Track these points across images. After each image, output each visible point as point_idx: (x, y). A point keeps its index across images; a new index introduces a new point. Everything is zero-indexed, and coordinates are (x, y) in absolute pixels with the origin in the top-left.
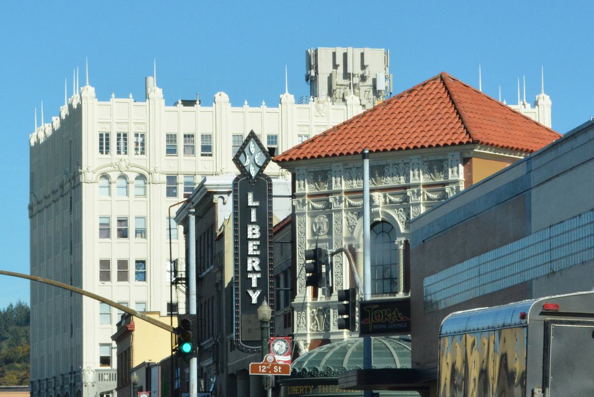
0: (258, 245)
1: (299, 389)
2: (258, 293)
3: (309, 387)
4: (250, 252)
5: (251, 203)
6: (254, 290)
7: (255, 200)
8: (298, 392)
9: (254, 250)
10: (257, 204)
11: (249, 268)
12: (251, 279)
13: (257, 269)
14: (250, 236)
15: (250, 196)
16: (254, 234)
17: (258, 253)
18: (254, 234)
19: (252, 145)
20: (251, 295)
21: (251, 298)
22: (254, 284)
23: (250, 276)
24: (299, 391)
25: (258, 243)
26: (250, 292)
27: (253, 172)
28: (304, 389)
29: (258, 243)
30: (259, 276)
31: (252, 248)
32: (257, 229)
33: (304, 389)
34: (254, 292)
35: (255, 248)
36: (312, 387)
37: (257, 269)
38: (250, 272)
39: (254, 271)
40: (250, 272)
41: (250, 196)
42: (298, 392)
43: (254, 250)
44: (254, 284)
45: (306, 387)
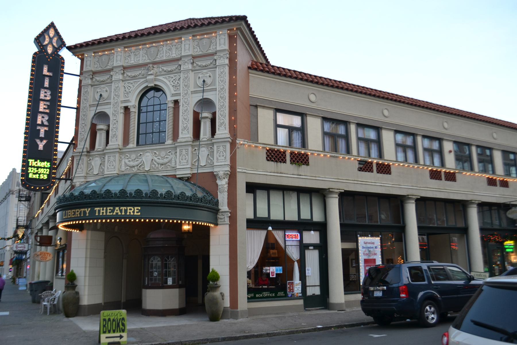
0: (48, 105)
1: (75, 212)
2: (45, 142)
3: (86, 209)
4: (41, 109)
5: (45, 71)
6: (42, 139)
7: (48, 71)
8: (73, 215)
9: (44, 108)
10: (51, 74)
11: (39, 122)
12: (39, 130)
13: (46, 123)
14: (42, 96)
16: (45, 96)
17: (47, 111)
18: (45, 96)
19: (52, 33)
21: (38, 146)
22: (42, 135)
23: (38, 128)
24: (75, 214)
25: (48, 103)
26: (38, 141)
27: (50, 50)
28: (81, 212)
29: (48, 103)
30: (46, 129)
31: (42, 107)
32: (49, 93)
33: (81, 212)
34: (41, 141)
36: (89, 209)
37: (46, 123)
38: (39, 125)
39: (42, 125)
42: (73, 215)
44: (42, 135)
45: (82, 210)
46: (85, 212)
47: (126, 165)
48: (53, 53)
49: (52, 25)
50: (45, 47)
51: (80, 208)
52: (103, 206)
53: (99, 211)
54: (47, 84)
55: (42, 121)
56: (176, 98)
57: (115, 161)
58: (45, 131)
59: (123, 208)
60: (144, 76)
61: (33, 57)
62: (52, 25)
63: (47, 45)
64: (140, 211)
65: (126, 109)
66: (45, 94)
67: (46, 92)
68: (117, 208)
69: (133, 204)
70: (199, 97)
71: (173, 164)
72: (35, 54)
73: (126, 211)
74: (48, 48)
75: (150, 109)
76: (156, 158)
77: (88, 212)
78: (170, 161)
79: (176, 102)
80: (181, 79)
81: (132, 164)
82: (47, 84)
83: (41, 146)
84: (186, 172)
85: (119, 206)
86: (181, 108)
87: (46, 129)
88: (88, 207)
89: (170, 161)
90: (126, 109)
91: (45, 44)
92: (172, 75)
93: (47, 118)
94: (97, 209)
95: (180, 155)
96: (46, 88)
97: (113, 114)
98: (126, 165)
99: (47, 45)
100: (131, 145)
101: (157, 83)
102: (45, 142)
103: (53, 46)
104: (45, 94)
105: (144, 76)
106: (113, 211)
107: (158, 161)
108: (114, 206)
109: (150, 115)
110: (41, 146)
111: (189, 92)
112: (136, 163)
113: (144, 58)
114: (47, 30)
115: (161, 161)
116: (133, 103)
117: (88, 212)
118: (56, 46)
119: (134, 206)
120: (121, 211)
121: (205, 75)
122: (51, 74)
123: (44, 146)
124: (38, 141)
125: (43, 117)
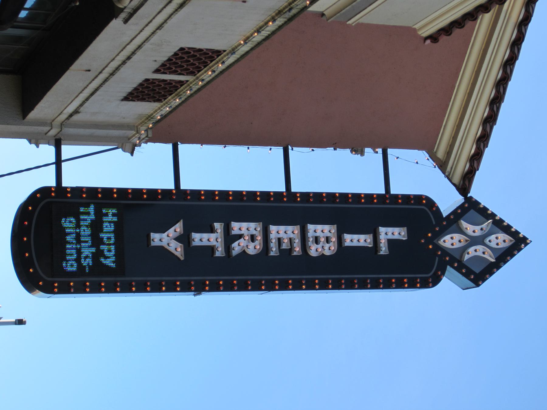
0: (291, 250)
2: (177, 249)
5: (389, 233)
6: (184, 239)
7: (391, 242)
9: (279, 240)
10: (384, 249)
11: (236, 227)
12: (212, 230)
13: (237, 247)
15: (398, 233)
17: (274, 251)
20: (171, 231)
21: (163, 229)
22: (200, 239)
25: (297, 249)
26: (178, 228)
27: (450, 241)
30: (220, 252)
31: (284, 233)
32: (329, 249)
34: (177, 239)
35: (284, 246)
37: (237, 247)
38: (227, 229)
39: (230, 238)
40: (227, 229)
41: (398, 233)
43: (279, 240)
44: (200, 239)
48: (445, 252)
49: (519, 242)
50: (454, 226)
54: (353, 240)
55: (240, 236)
58: (212, 249)
61: (419, 198)
62: (519, 242)
63: (461, 231)
66: (323, 239)
67: (328, 240)
72: (430, 203)
74: (457, 237)
82: (353, 240)
83: (167, 240)
87: (220, 252)
91: (464, 224)
93: (253, 249)
96: (340, 240)
99: (461, 231)
102: (177, 249)
103: (464, 249)
104: (323, 239)
110: (167, 240)
114: (501, 226)
118: (466, 257)
122: (384, 249)
123: (162, 251)
124: (178, 228)
125: (253, 238)
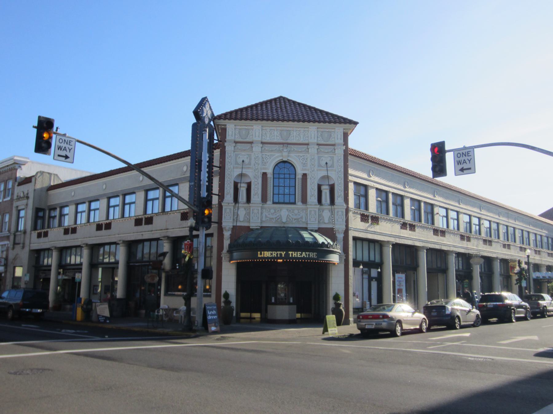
45: (279, 252)
46: (281, 254)
47: (266, 217)
51: (276, 251)
52: (295, 251)
53: (292, 254)
56: (305, 172)
57: (258, 213)
59: (307, 253)
60: (281, 151)
64: (316, 255)
65: (264, 175)
68: (304, 253)
69: (313, 251)
70: (324, 173)
71: (304, 220)
73: (309, 255)
75: (282, 176)
76: (290, 214)
77: (283, 254)
78: (302, 218)
79: (305, 175)
80: (309, 160)
81: (271, 216)
84: (316, 227)
85: (305, 252)
86: (308, 180)
88: (283, 252)
89: (302, 218)
90: (264, 175)
92: (301, 155)
94: (290, 253)
95: (310, 214)
97: (254, 177)
98: (266, 217)
100: (268, 202)
101: (290, 159)
105: (281, 151)
106: (301, 254)
107: (292, 216)
108: (302, 252)
109: (282, 181)
111: (316, 170)
112: (274, 216)
113: (278, 138)
115: (295, 217)
116: (269, 171)
117: (283, 254)
119: (313, 252)
120: (306, 255)
121: (326, 158)
